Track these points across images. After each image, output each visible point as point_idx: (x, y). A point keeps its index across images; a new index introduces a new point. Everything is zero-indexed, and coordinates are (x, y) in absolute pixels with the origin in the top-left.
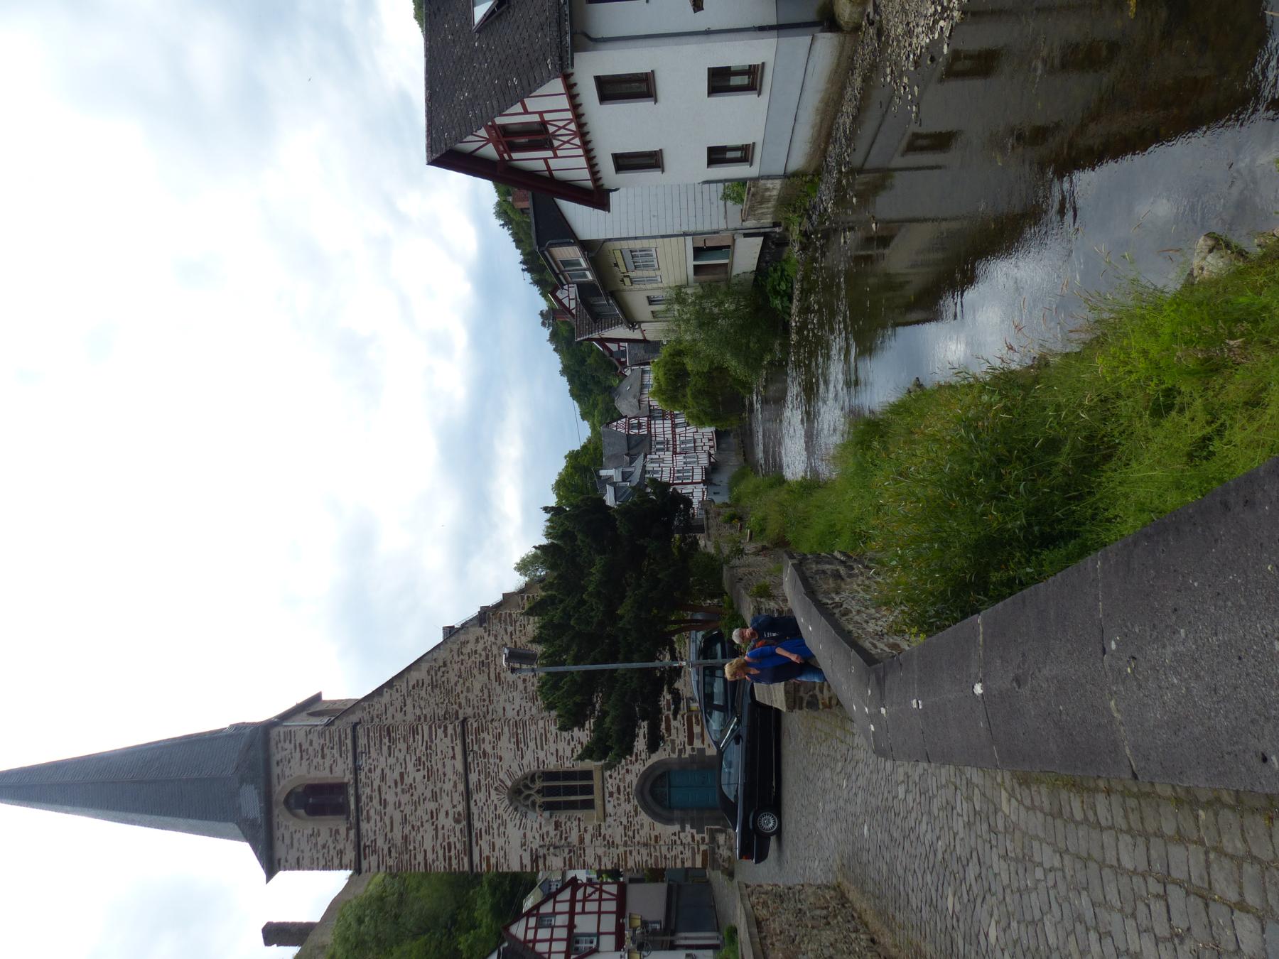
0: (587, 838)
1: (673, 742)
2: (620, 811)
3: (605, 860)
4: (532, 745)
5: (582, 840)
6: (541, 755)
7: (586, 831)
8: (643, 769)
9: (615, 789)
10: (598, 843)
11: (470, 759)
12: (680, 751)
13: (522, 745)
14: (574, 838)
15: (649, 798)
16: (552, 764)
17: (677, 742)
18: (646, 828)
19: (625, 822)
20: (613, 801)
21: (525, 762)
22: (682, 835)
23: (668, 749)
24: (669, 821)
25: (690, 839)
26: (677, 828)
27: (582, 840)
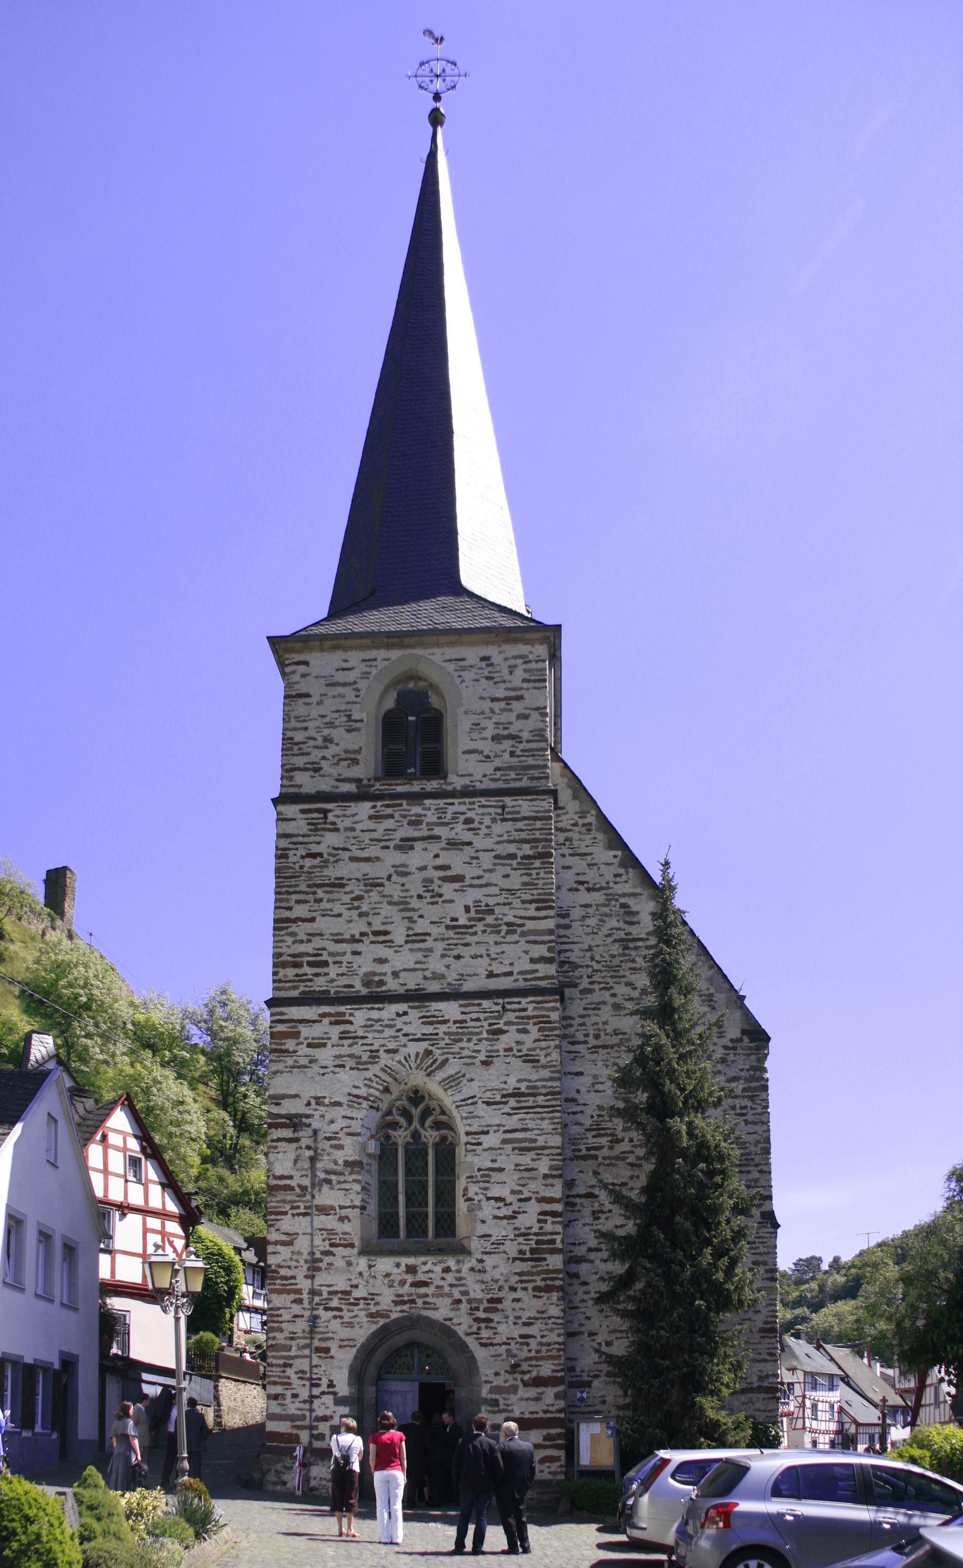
0: (330, 1222)
1: (514, 1389)
2: (379, 1286)
3: (285, 1252)
4: (513, 1122)
5: (325, 1210)
6: (491, 1140)
7: (342, 1219)
8: (461, 1331)
9: (421, 1277)
10: (318, 1241)
11: (486, 1004)
12: (495, 1403)
13: (512, 1102)
14: (326, 1197)
15: (400, 1339)
16: (469, 1162)
17: (513, 1398)
18: (345, 1333)
19: (357, 1293)
20: (398, 1274)
21: (481, 1109)
22: (329, 1399)
23: (499, 1381)
24: (357, 1374)
25: (320, 1412)
26: (343, 1389)
27: (325, 1210)
